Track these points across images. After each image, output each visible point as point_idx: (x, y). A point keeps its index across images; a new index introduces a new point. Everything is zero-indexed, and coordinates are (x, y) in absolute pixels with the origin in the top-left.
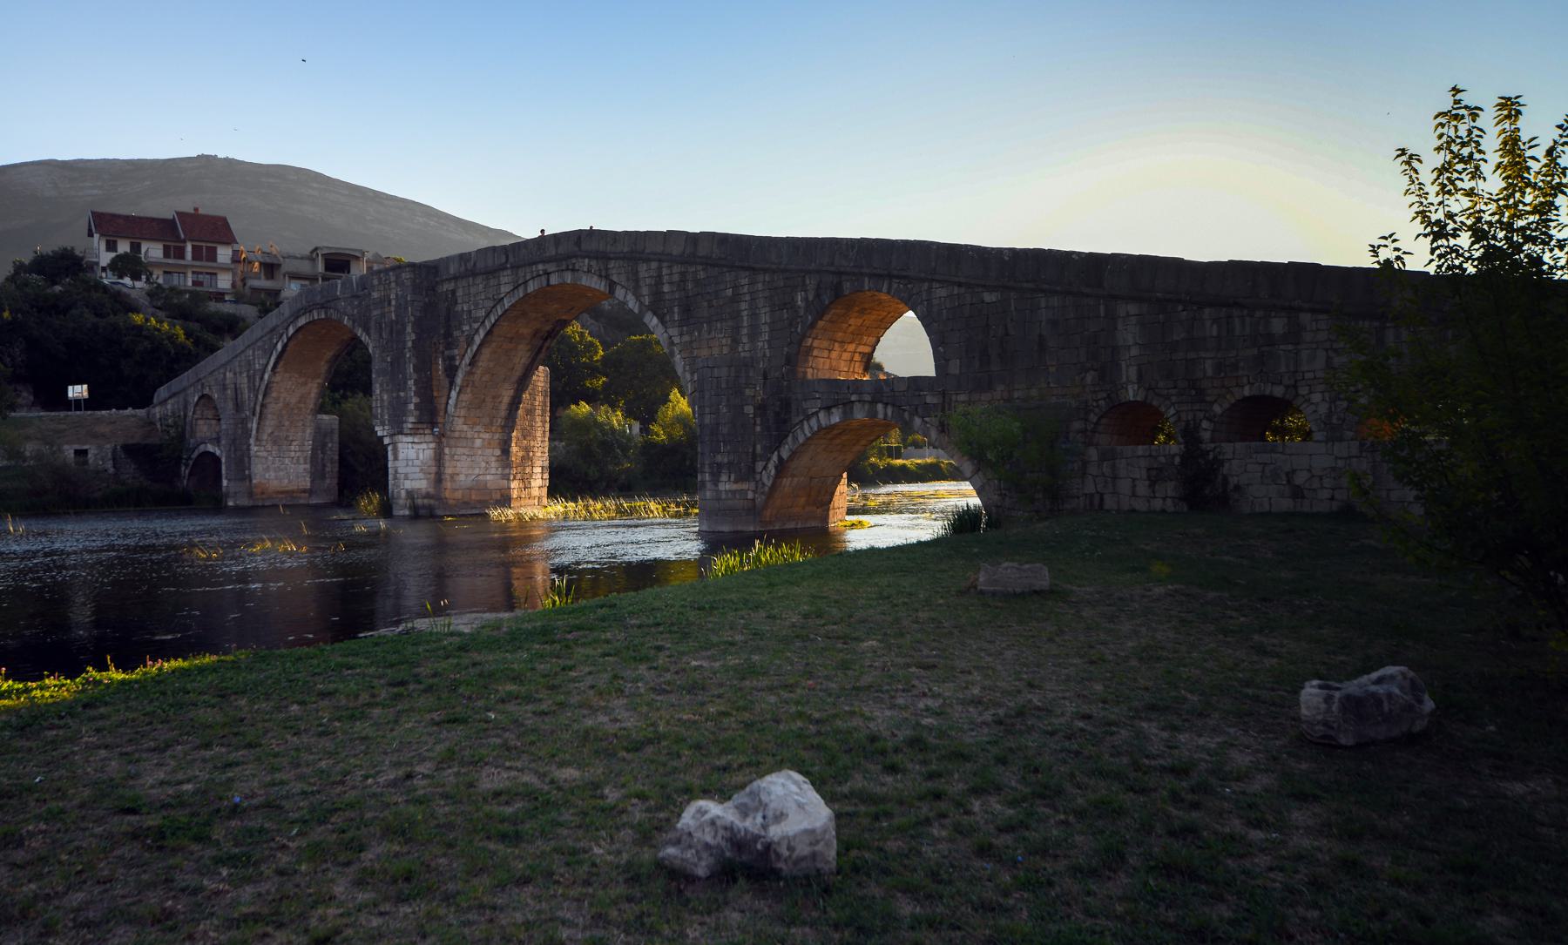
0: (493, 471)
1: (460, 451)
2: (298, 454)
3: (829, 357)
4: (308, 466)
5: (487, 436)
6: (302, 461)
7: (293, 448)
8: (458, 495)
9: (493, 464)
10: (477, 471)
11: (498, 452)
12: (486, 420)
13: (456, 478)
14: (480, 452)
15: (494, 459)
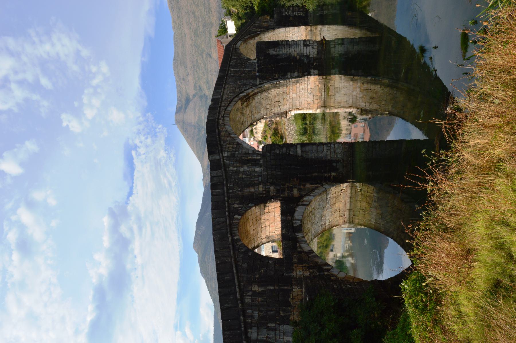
0: (306, 85)
1: (298, 103)
2: (291, 33)
3: (269, 226)
4: (296, 27)
5: (291, 93)
6: (294, 31)
7: (288, 35)
8: (316, 101)
9: (303, 86)
10: (306, 93)
11: (298, 85)
12: (285, 96)
13: (309, 102)
14: (298, 94)
15: (301, 86)
